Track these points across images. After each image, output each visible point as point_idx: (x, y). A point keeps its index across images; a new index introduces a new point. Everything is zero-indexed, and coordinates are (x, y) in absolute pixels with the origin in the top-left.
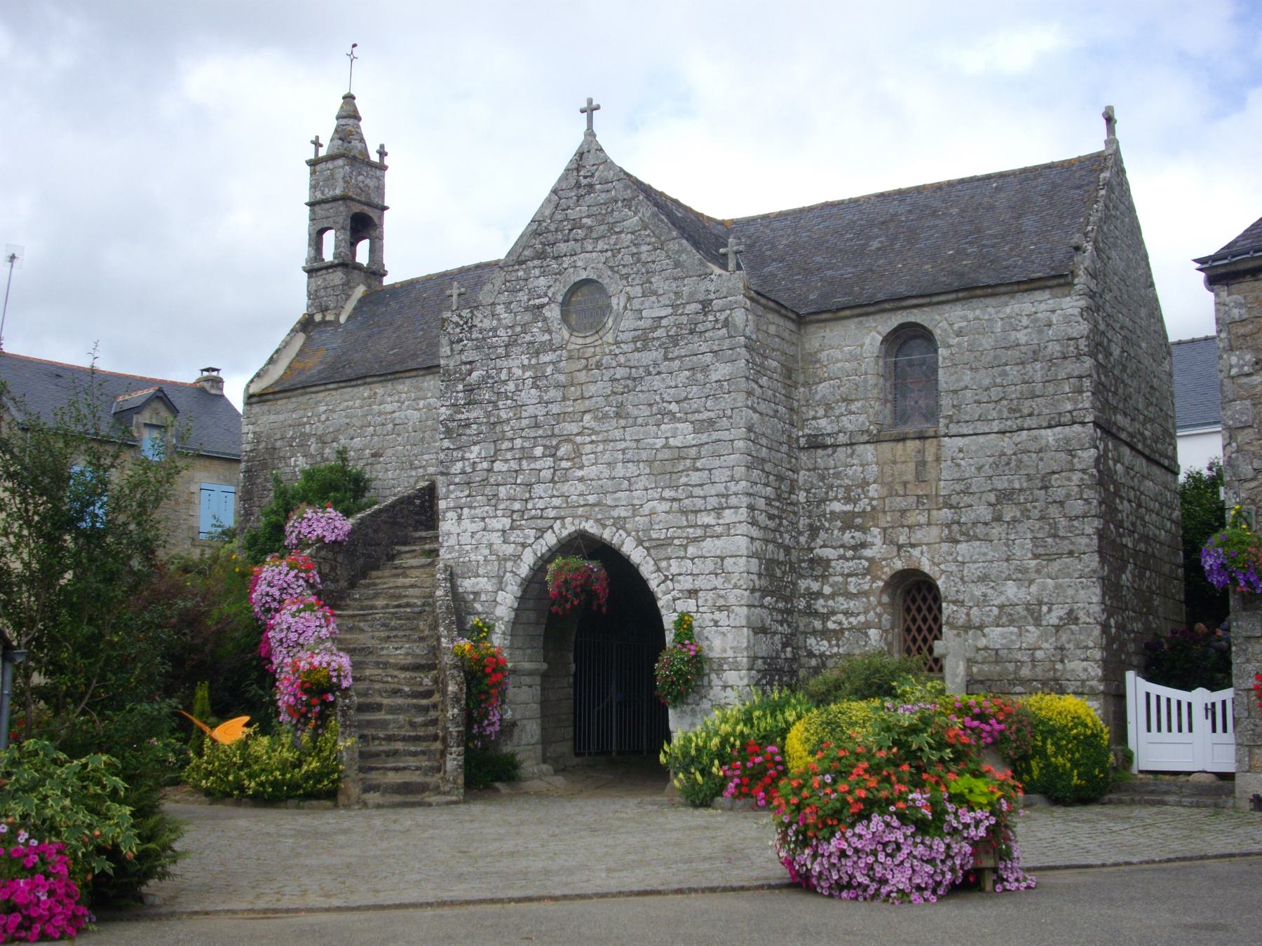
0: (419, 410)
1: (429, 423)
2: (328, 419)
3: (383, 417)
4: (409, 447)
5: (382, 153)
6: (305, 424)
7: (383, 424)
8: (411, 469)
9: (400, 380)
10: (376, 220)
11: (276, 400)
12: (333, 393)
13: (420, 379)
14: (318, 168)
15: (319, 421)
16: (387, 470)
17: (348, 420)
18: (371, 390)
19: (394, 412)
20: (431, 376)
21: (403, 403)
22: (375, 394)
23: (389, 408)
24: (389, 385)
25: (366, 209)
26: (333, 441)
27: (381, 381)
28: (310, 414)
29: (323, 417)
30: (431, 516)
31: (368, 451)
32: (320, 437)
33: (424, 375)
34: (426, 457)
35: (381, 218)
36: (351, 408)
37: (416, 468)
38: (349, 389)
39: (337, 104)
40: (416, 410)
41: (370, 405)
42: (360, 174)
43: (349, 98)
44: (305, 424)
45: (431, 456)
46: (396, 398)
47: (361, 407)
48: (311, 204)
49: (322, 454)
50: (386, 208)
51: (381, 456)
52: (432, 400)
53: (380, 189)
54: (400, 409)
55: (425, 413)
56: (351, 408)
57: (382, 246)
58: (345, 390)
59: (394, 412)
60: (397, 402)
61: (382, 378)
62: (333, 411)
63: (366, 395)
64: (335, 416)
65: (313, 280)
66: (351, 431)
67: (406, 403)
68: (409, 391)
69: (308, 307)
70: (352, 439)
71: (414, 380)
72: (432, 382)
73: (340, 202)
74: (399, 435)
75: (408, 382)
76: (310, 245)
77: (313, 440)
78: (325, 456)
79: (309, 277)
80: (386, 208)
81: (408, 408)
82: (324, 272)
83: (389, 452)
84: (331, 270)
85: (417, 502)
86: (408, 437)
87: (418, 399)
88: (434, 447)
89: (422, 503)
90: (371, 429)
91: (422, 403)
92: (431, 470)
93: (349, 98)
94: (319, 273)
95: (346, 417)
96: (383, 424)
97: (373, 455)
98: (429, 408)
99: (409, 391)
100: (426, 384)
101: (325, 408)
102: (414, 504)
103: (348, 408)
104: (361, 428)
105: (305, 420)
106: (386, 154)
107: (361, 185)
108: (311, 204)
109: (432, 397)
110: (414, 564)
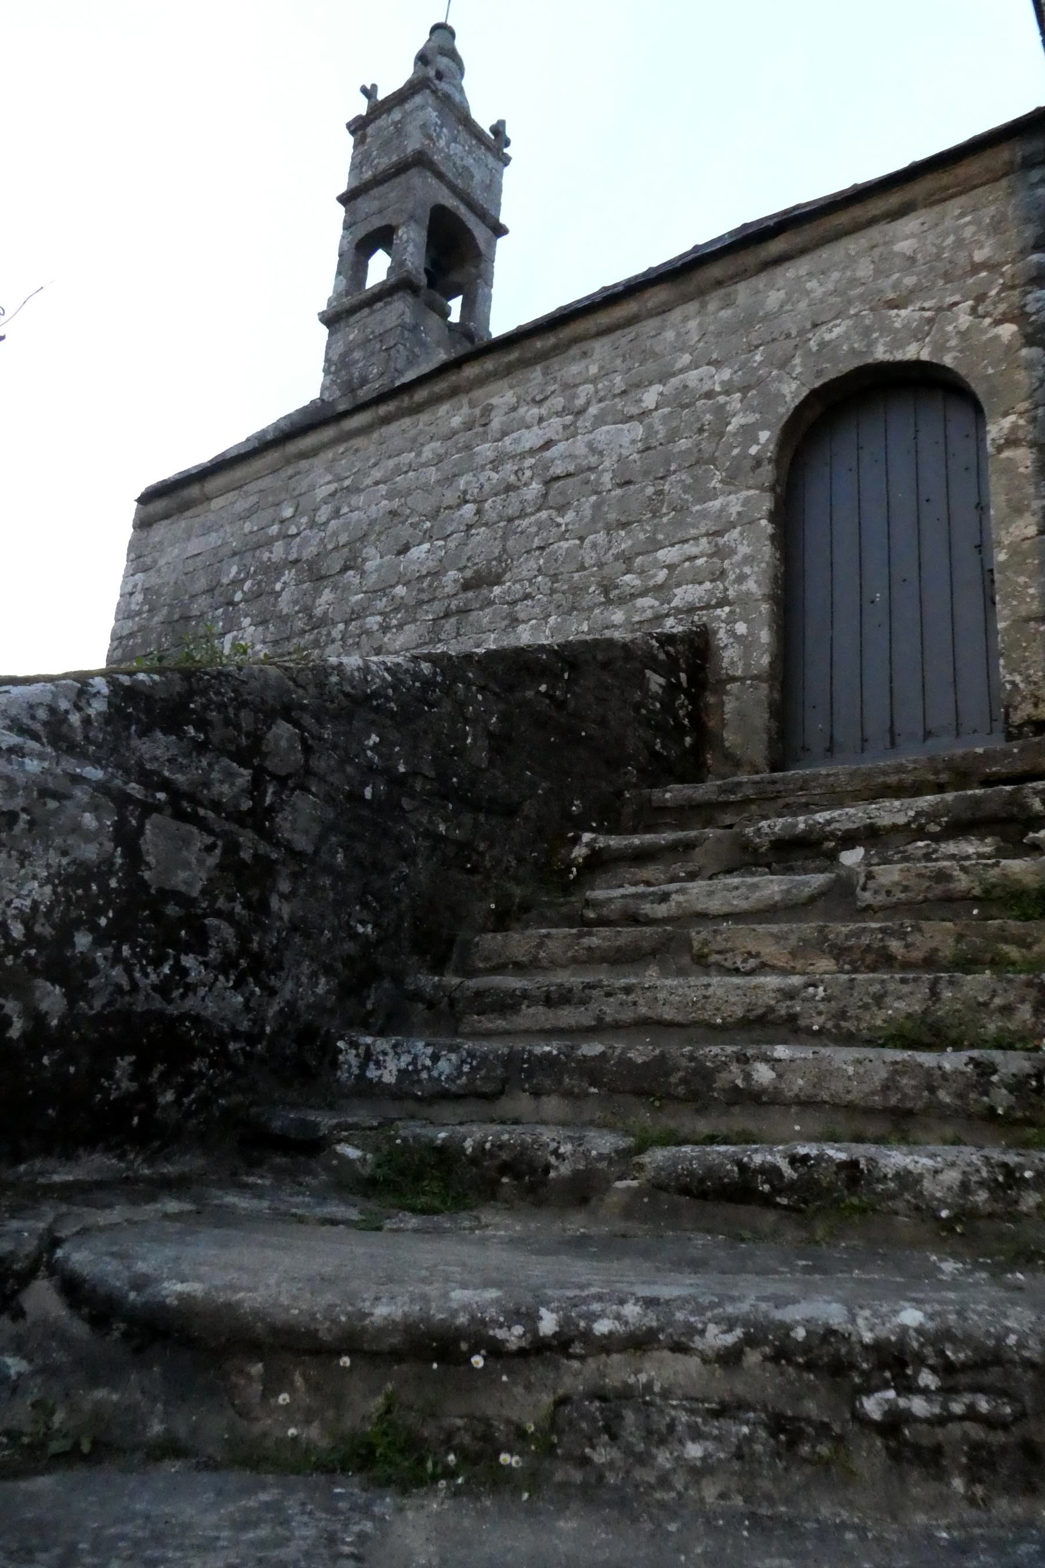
0: (645, 414)
1: (683, 444)
2: (336, 514)
3: (509, 467)
4: (601, 537)
5: (498, 130)
6: (272, 540)
7: (509, 488)
8: (609, 602)
9: (574, 351)
10: (482, 245)
11: (208, 499)
12: (359, 442)
13: (649, 326)
14: (370, 130)
15: (312, 524)
16: (515, 621)
17: (396, 503)
18: (472, 405)
19: (548, 444)
20: (692, 307)
21: (580, 412)
22: (488, 410)
23: (531, 438)
24: (536, 374)
25: (463, 211)
26: (345, 569)
27: (509, 370)
28: (288, 512)
29: (322, 515)
30: (697, 750)
31: (452, 574)
32: (312, 564)
33: (663, 310)
34: (668, 555)
35: (492, 246)
36: (410, 467)
37: (626, 599)
38: (406, 422)
39: (420, 39)
40: (630, 418)
41: (468, 447)
42: (455, 140)
43: (442, 31)
44: (270, 542)
45: (690, 549)
46: (558, 402)
47: (439, 460)
48: (345, 199)
49: (307, 610)
50: (500, 230)
51: (498, 580)
52: (692, 377)
53: (494, 188)
54: (570, 432)
55: (665, 419)
56: (410, 467)
57: (489, 298)
58: (393, 428)
59: (548, 444)
60: (558, 414)
61: (514, 355)
62: (354, 490)
63: (456, 421)
64: (359, 500)
65: (339, 335)
66: (404, 532)
67: (593, 410)
68: (605, 373)
69: (324, 388)
70: (405, 549)
71: (623, 338)
72: (693, 324)
73: (413, 171)
74: (562, 509)
75: (600, 348)
76: (339, 273)
77: (288, 576)
78: (318, 612)
79: (330, 335)
80: (500, 230)
81: (600, 420)
82: (366, 311)
83: (528, 566)
84: (380, 304)
85: (656, 681)
86: (597, 507)
87: (638, 386)
88: (704, 515)
89: (672, 689)
90: (469, 509)
91: (650, 397)
92: (685, 594)
93: (442, 31)
94: (357, 316)
95: (390, 496)
96: (509, 488)
97: (466, 586)
98: (682, 400)
99: (605, 373)
100: (670, 335)
101: (332, 487)
102: (643, 684)
103: (398, 471)
104: (434, 515)
105: (274, 529)
106: (507, 143)
107: (458, 162)
108: (345, 199)
109: (695, 365)
110: (715, 905)
